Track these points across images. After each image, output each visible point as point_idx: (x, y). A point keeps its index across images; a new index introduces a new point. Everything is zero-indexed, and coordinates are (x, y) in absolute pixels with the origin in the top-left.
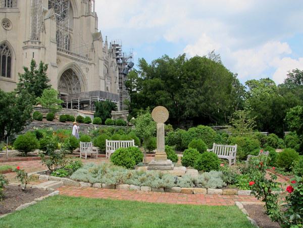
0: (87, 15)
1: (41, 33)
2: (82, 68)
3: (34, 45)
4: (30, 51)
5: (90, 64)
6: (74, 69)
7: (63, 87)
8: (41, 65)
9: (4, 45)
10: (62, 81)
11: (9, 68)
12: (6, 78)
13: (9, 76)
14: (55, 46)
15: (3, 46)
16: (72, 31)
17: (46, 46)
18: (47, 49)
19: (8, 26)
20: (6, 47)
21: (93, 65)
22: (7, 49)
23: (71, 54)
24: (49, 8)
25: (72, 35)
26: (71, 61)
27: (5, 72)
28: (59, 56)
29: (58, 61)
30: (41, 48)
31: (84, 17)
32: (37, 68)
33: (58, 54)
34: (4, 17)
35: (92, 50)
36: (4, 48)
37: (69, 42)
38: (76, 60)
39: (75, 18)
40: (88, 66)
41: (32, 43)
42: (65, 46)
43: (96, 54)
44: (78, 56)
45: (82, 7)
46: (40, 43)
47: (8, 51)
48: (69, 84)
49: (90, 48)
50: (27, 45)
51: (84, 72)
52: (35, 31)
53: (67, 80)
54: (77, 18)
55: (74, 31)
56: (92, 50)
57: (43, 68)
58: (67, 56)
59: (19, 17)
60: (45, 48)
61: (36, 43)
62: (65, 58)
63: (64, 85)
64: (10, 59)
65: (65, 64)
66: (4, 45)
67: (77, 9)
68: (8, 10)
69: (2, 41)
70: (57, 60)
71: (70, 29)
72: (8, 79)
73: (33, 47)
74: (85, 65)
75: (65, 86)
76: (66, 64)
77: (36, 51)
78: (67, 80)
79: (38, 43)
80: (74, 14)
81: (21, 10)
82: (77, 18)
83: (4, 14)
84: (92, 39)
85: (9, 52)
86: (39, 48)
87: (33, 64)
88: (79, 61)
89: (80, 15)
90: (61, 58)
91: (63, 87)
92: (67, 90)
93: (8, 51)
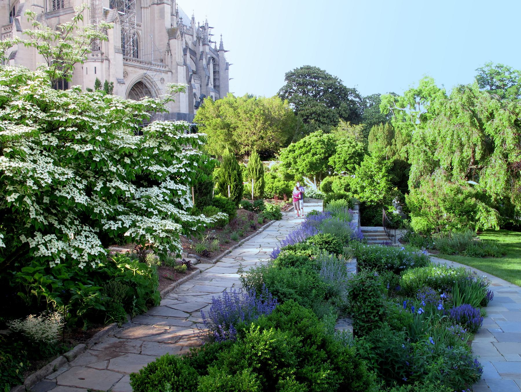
0: (159, 2)
2: (154, 80)
6: (144, 82)
14: (121, 56)
16: (140, 26)
18: (111, 61)
21: (170, 73)
23: (141, 63)
24: (111, 7)
25: (140, 32)
26: (142, 72)
28: (126, 67)
29: (126, 74)
30: (104, 61)
31: (155, 5)
33: (124, 65)
35: (168, 52)
37: (136, 43)
39: (144, 7)
40: (163, 75)
41: (93, 56)
42: (132, 52)
43: (173, 58)
44: (151, 64)
46: (102, 54)
49: (165, 49)
51: (158, 83)
54: (147, 8)
56: (168, 52)
58: (134, 67)
60: (109, 61)
65: (135, 75)
71: (137, 25)
77: (98, 65)
79: (100, 55)
82: (147, 8)
83: (57, 18)
84: (168, 37)
89: (149, 4)
90: (129, 69)
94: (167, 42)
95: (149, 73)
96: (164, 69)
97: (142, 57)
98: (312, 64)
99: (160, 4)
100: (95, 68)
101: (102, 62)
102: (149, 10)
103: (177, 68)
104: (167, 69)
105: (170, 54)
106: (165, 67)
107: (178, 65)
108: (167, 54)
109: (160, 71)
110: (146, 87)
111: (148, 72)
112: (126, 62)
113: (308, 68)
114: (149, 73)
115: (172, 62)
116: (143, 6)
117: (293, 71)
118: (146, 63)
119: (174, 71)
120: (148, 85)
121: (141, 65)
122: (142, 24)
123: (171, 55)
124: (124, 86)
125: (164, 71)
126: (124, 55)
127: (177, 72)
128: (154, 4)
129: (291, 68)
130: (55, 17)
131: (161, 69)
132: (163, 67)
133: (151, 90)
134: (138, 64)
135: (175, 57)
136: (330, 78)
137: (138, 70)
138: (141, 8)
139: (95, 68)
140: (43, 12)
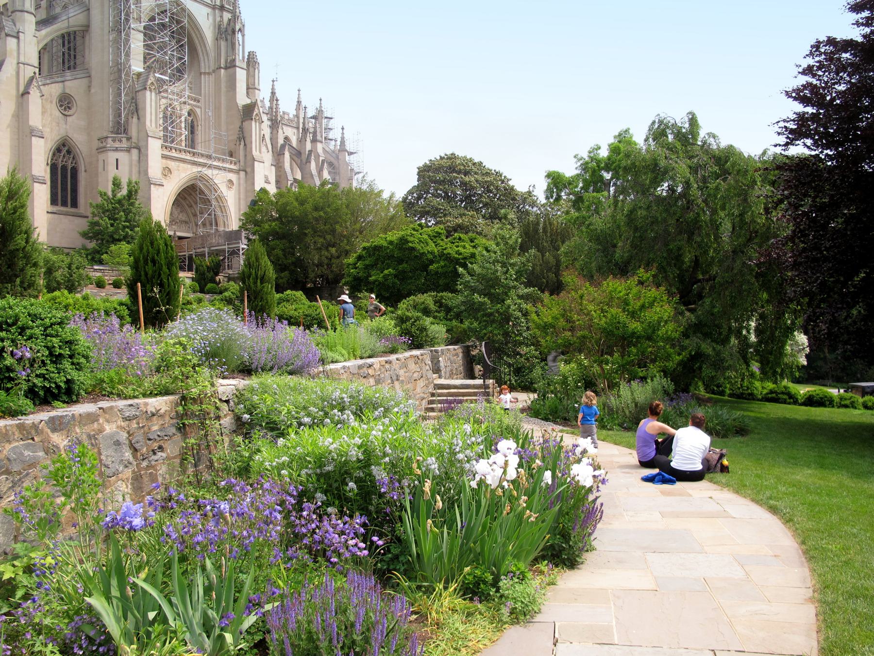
0: (228, 65)
1: (130, 119)
3: (117, 145)
4: (112, 156)
7: (182, 222)
9: (64, 145)
10: (179, 210)
11: (75, 191)
12: (69, 209)
13: (75, 204)
17: (140, 144)
19: (69, 108)
20: (66, 148)
22: (69, 152)
23: (194, 154)
25: (198, 111)
26: (196, 169)
27: (66, 197)
29: (167, 172)
32: (124, 192)
34: (60, 91)
36: (65, 150)
38: (204, 165)
39: (205, 73)
41: (114, 141)
42: (183, 137)
43: (248, 149)
44: (209, 157)
45: (218, 48)
47: (72, 156)
49: (235, 137)
52: (120, 116)
53: (191, 206)
55: (202, 101)
56: (240, 141)
59: (89, 87)
61: (121, 141)
62: (182, 165)
63: (183, 217)
64: (75, 171)
67: (207, 54)
68: (68, 74)
69: (59, 138)
70: (164, 169)
72: (73, 210)
73: (116, 150)
74: (222, 173)
75: (187, 219)
76: (183, 175)
78: (191, 206)
79: (124, 140)
80: (202, 64)
81: (93, 73)
82: (209, 74)
83: (61, 85)
84: (240, 117)
85: (74, 158)
86: (128, 150)
87: (117, 184)
88: (210, 167)
90: (172, 164)
91: (182, 222)
93: (72, 156)
94: (238, 124)
95: (209, 172)
96: (232, 167)
97: (199, 149)
98: (461, 152)
99: (229, 68)
100: (117, 160)
102: (212, 78)
108: (238, 143)
109: (225, 169)
111: (205, 169)
112: (167, 153)
113: (452, 157)
114: (209, 172)
116: (203, 71)
117: (428, 163)
119: (248, 170)
122: (202, 98)
123: (245, 145)
124: (161, 188)
126: (165, 141)
128: (221, 68)
129: (423, 160)
130: (58, 82)
131: (227, 165)
133: (212, 197)
134: (188, 157)
135: (251, 148)
136: (488, 174)
137: (190, 166)
138: (201, 74)
139: (117, 160)
140: (35, 73)
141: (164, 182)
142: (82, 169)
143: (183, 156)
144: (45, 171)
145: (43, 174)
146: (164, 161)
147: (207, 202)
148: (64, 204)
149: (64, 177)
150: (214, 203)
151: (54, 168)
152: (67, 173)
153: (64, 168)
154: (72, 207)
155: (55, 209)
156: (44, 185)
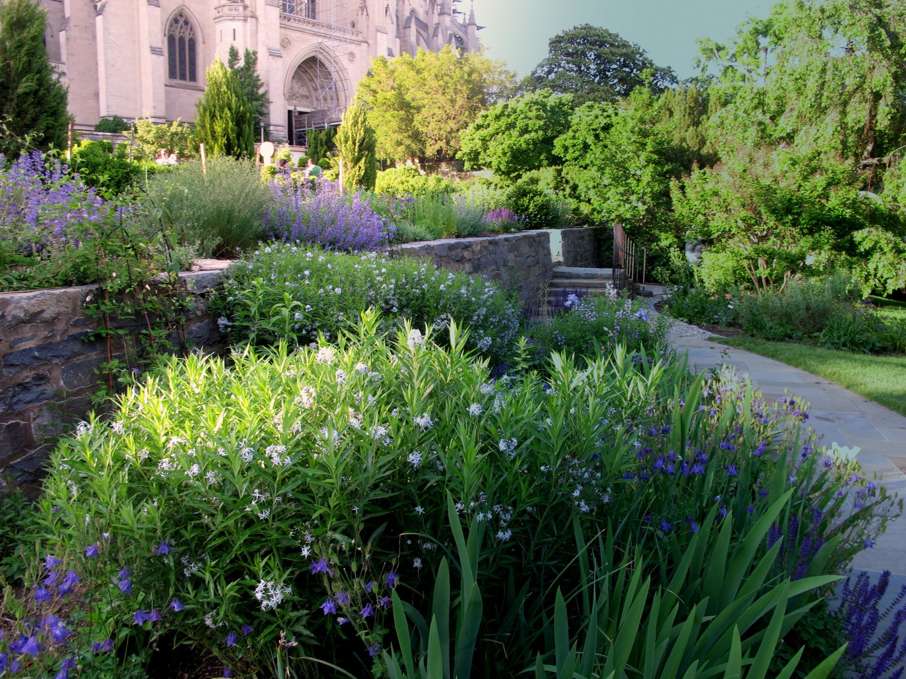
2: (338, 54)
3: (234, 12)
5: (359, 43)
6: (320, 57)
7: (303, 96)
8: (247, 55)
10: (299, 84)
11: (193, 63)
12: (188, 83)
13: (193, 77)
15: (179, 18)
18: (260, 19)
20: (183, 19)
21: (364, 45)
22: (186, 23)
26: (316, 40)
27: (185, 69)
28: (288, 32)
29: (285, 43)
32: (241, 63)
33: (282, 27)
35: (362, 11)
40: (352, 48)
44: (329, 27)
46: (245, 7)
48: (316, 90)
50: (221, 14)
51: (344, 61)
53: (312, 80)
56: (362, 11)
57: (251, 60)
58: (303, 31)
63: (304, 91)
64: (193, 44)
65: (303, 47)
66: (181, 15)
69: (175, 7)
74: (344, 45)
75: (308, 94)
76: (303, 46)
77: (238, 25)
78: (312, 80)
79: (241, 8)
87: (234, 54)
90: (293, 35)
91: (303, 96)
92: (312, 102)
95: (328, 43)
96: (354, 38)
97: (321, 17)
101: (245, 21)
103: (376, 37)
104: (360, 38)
105: (365, 13)
106: (357, 35)
107: (378, 31)
108: (360, 13)
110: (322, 65)
112: (285, 22)
114: (328, 43)
115: (368, 26)
118: (323, 26)
119: (371, 42)
120: (327, 64)
121: (313, 29)
124: (280, 61)
125: (352, 42)
126: (285, 11)
127: (376, 42)
132: (353, 34)
133: (332, 69)
134: (309, 27)
137: (309, 37)
141: (283, 53)
142: (200, 39)
143: (304, 26)
144: (163, 42)
145: (159, 45)
146: (283, 31)
147: (327, 75)
148: (183, 77)
149: (182, 49)
150: (335, 76)
151: (171, 39)
152: (184, 44)
153: (182, 39)
154: (190, 80)
155: (174, 82)
156: (162, 58)
